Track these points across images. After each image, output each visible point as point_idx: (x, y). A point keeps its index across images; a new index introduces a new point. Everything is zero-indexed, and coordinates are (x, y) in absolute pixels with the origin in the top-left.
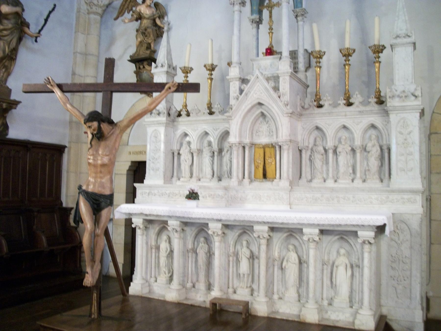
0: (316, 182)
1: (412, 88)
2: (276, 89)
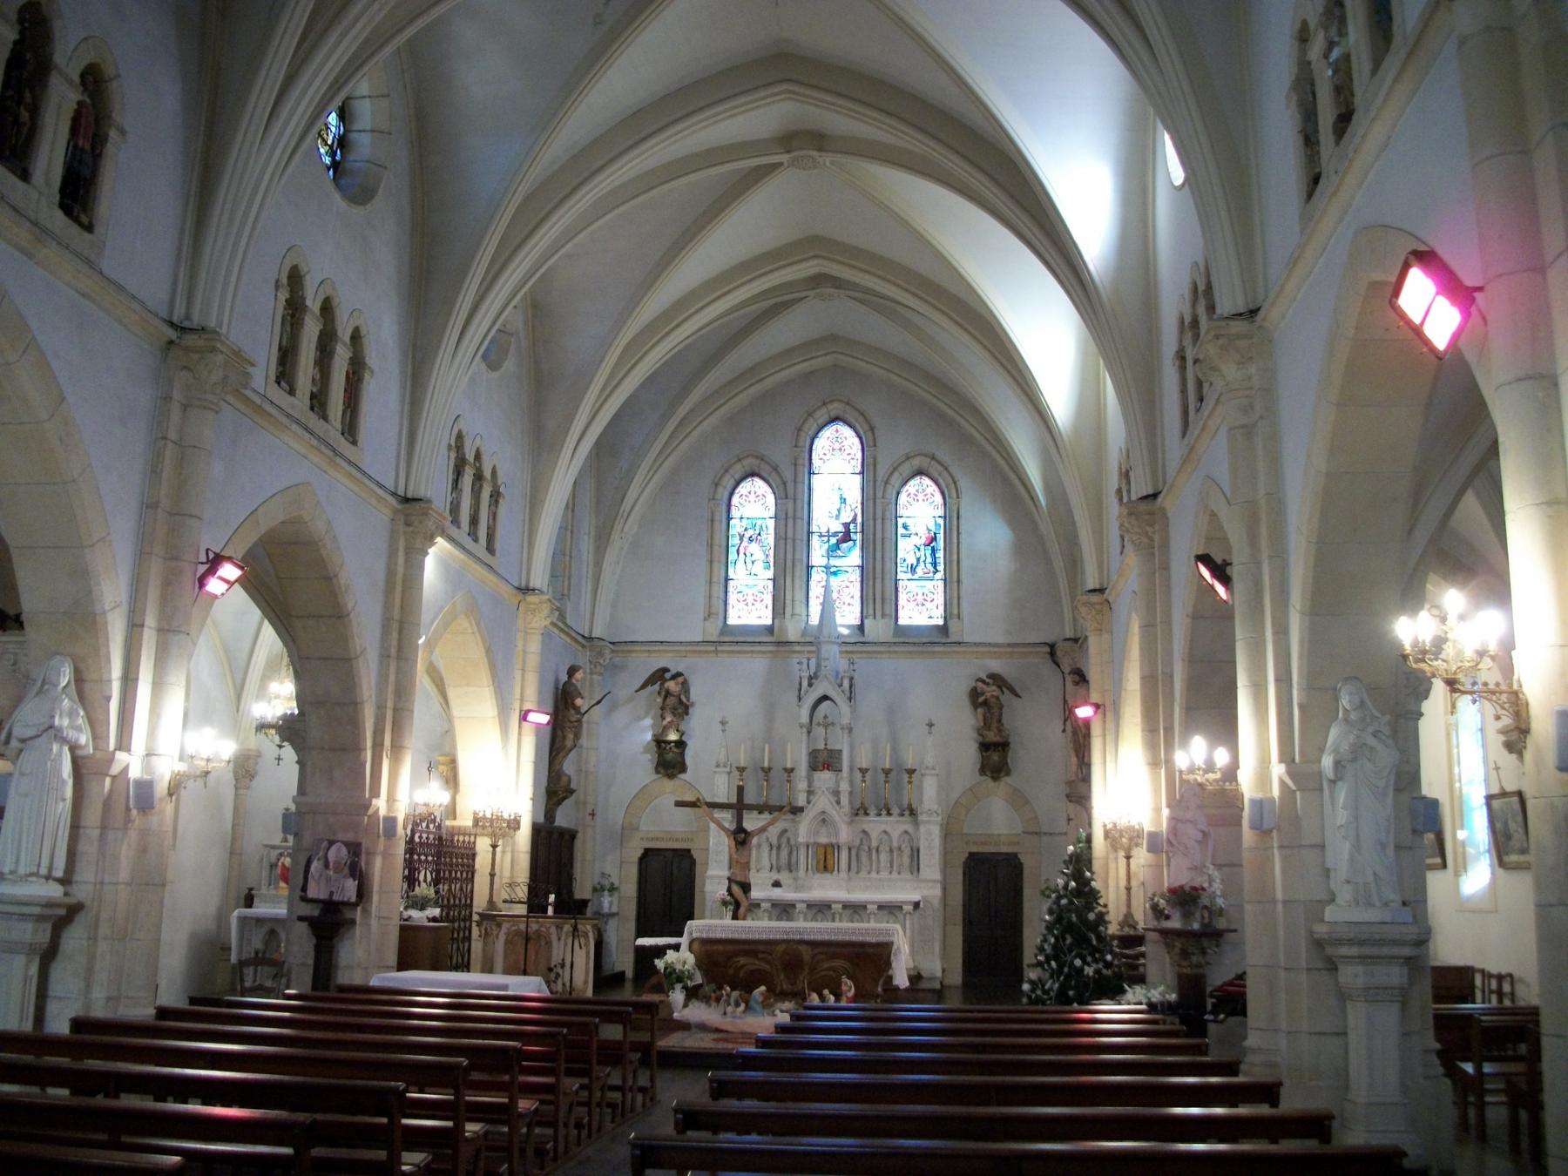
0: (863, 874)
1: (935, 807)
2: (838, 803)
